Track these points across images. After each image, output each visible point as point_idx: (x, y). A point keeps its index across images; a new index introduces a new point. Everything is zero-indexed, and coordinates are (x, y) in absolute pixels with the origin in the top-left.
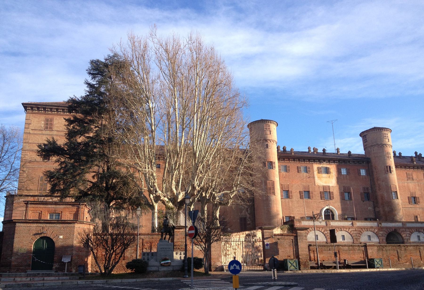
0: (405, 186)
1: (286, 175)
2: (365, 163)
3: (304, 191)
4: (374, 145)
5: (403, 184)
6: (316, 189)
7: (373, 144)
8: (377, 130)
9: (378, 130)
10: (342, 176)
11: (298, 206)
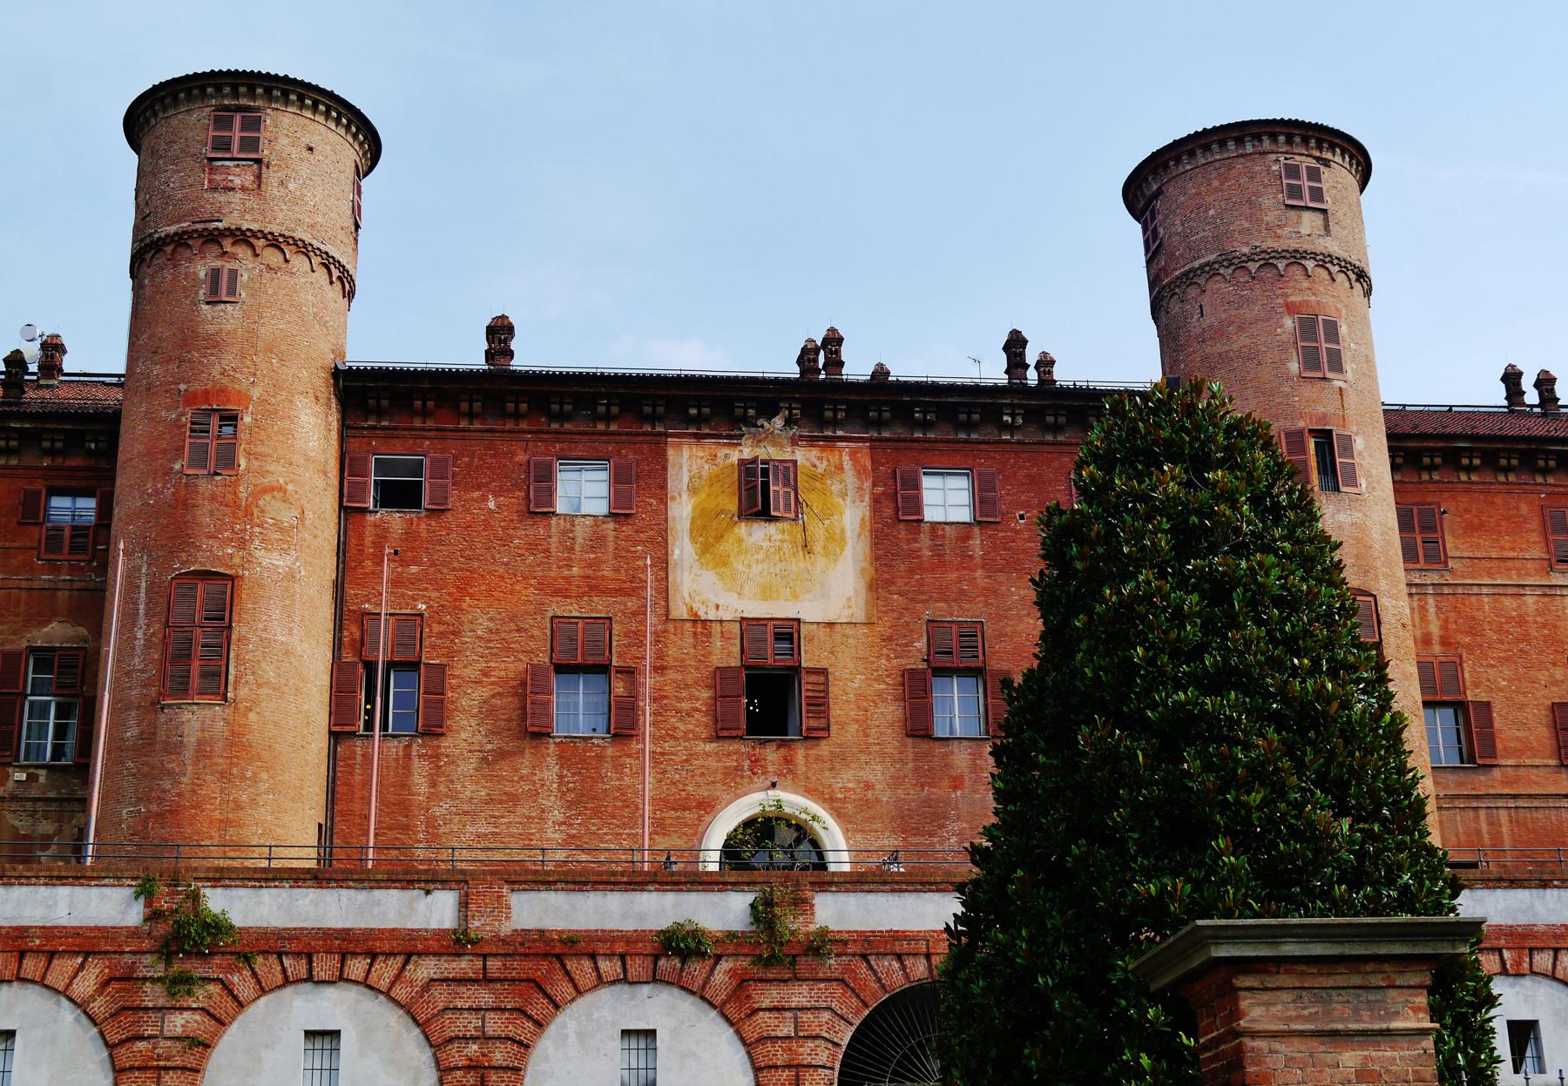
0: (1521, 621)
1: (410, 535)
4: (1202, 267)
5: (1508, 602)
6: (680, 647)
7: (1196, 264)
8: (1231, 145)
9: (1240, 141)
10: (925, 540)
11: (490, 801)
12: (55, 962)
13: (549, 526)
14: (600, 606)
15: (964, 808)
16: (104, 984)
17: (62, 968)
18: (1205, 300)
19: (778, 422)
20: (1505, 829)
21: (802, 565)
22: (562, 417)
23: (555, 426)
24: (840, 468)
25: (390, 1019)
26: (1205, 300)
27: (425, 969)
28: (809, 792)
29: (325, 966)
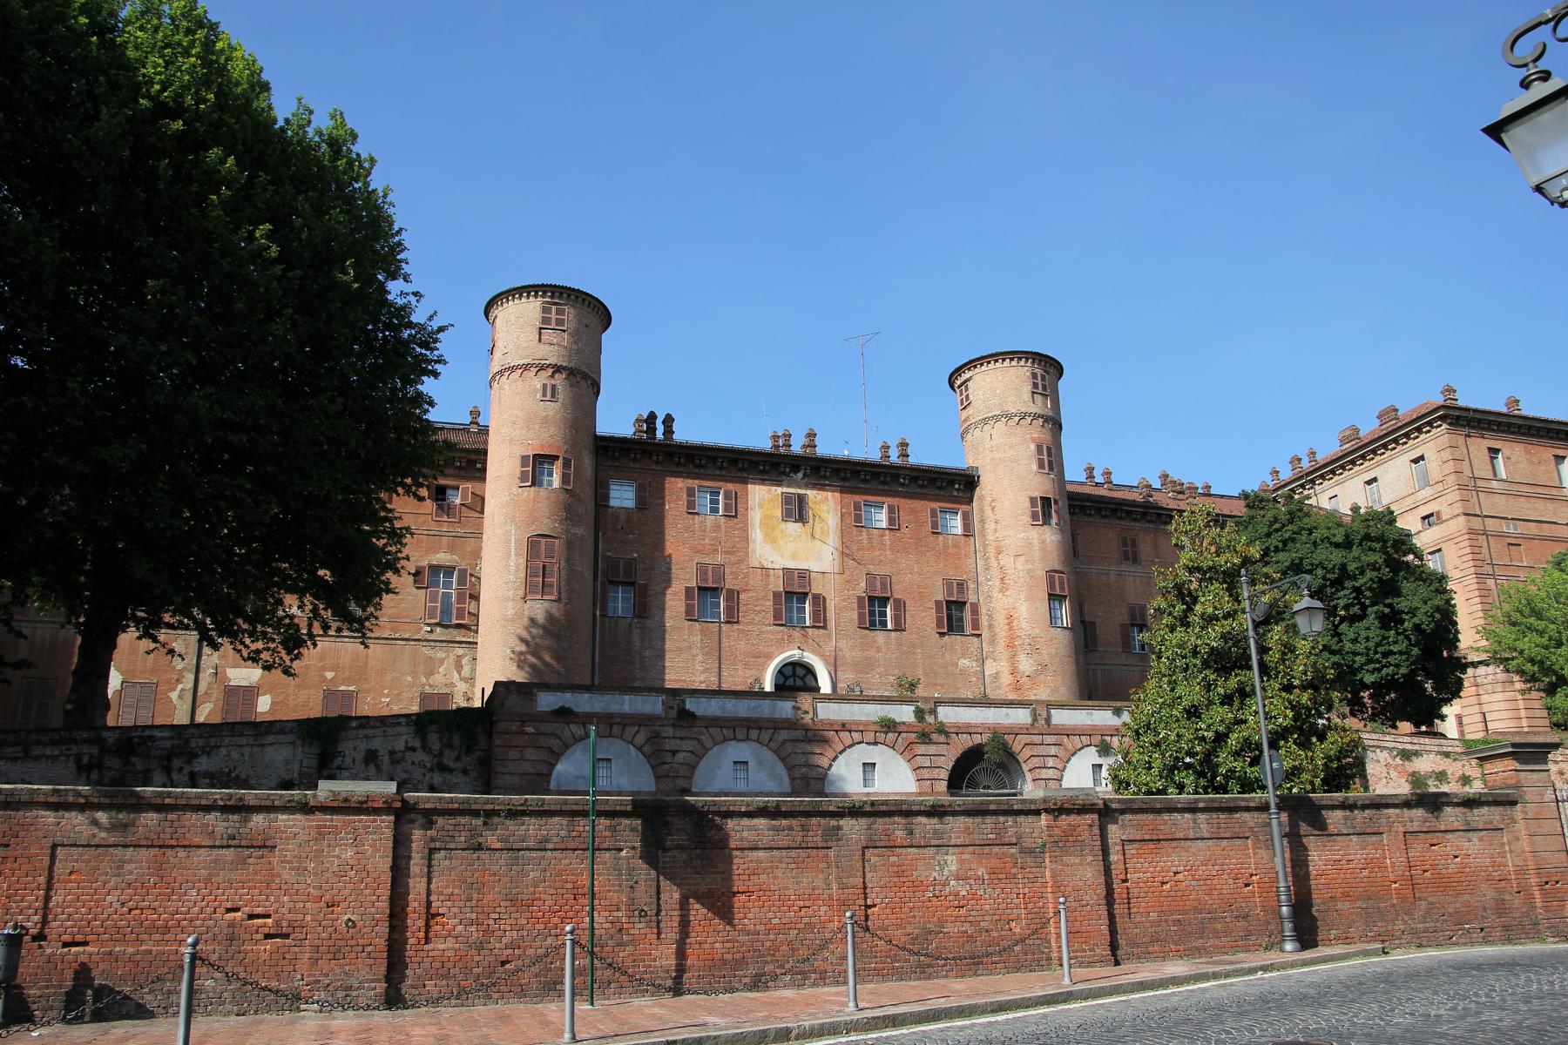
2: (957, 486)
3: (700, 588)
6: (755, 580)
7: (990, 415)
12: (627, 729)
13: (693, 519)
14: (719, 559)
15: (882, 662)
16: (648, 740)
17: (631, 730)
18: (993, 432)
19: (800, 475)
20: (1099, 679)
21: (810, 544)
22: (700, 466)
23: (697, 470)
24: (827, 499)
25: (769, 755)
26: (993, 432)
27: (784, 735)
28: (813, 652)
29: (740, 733)
